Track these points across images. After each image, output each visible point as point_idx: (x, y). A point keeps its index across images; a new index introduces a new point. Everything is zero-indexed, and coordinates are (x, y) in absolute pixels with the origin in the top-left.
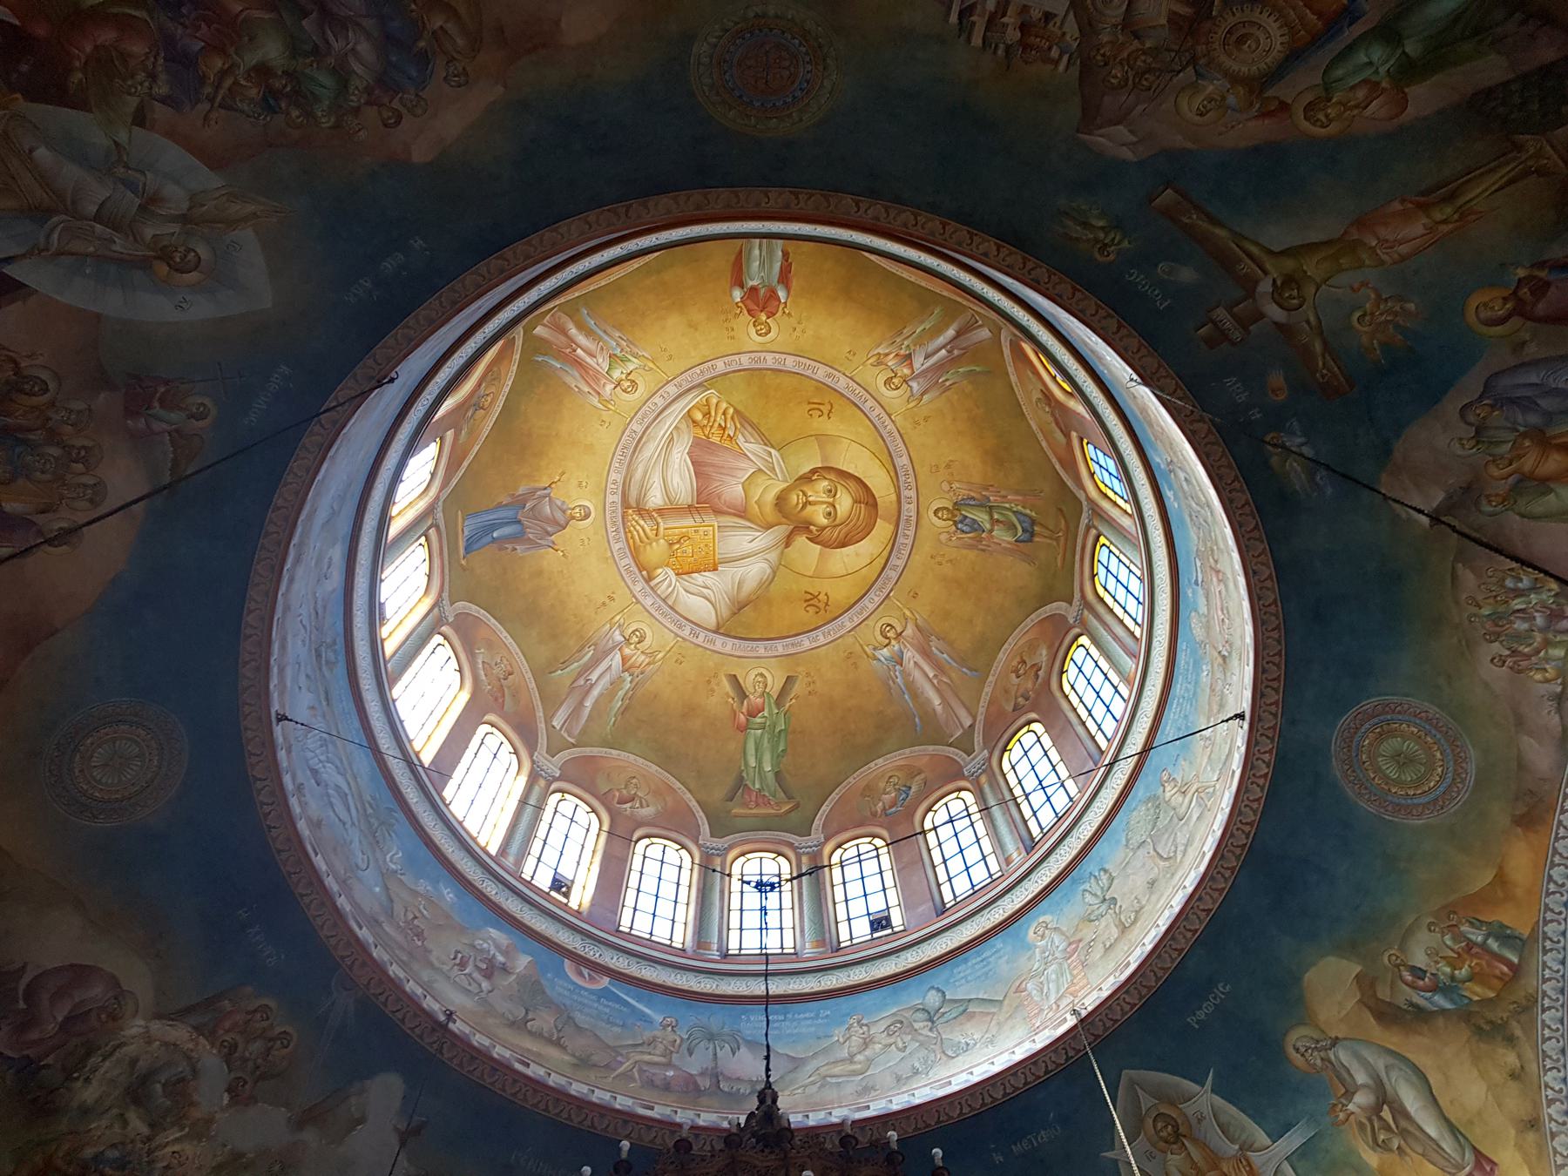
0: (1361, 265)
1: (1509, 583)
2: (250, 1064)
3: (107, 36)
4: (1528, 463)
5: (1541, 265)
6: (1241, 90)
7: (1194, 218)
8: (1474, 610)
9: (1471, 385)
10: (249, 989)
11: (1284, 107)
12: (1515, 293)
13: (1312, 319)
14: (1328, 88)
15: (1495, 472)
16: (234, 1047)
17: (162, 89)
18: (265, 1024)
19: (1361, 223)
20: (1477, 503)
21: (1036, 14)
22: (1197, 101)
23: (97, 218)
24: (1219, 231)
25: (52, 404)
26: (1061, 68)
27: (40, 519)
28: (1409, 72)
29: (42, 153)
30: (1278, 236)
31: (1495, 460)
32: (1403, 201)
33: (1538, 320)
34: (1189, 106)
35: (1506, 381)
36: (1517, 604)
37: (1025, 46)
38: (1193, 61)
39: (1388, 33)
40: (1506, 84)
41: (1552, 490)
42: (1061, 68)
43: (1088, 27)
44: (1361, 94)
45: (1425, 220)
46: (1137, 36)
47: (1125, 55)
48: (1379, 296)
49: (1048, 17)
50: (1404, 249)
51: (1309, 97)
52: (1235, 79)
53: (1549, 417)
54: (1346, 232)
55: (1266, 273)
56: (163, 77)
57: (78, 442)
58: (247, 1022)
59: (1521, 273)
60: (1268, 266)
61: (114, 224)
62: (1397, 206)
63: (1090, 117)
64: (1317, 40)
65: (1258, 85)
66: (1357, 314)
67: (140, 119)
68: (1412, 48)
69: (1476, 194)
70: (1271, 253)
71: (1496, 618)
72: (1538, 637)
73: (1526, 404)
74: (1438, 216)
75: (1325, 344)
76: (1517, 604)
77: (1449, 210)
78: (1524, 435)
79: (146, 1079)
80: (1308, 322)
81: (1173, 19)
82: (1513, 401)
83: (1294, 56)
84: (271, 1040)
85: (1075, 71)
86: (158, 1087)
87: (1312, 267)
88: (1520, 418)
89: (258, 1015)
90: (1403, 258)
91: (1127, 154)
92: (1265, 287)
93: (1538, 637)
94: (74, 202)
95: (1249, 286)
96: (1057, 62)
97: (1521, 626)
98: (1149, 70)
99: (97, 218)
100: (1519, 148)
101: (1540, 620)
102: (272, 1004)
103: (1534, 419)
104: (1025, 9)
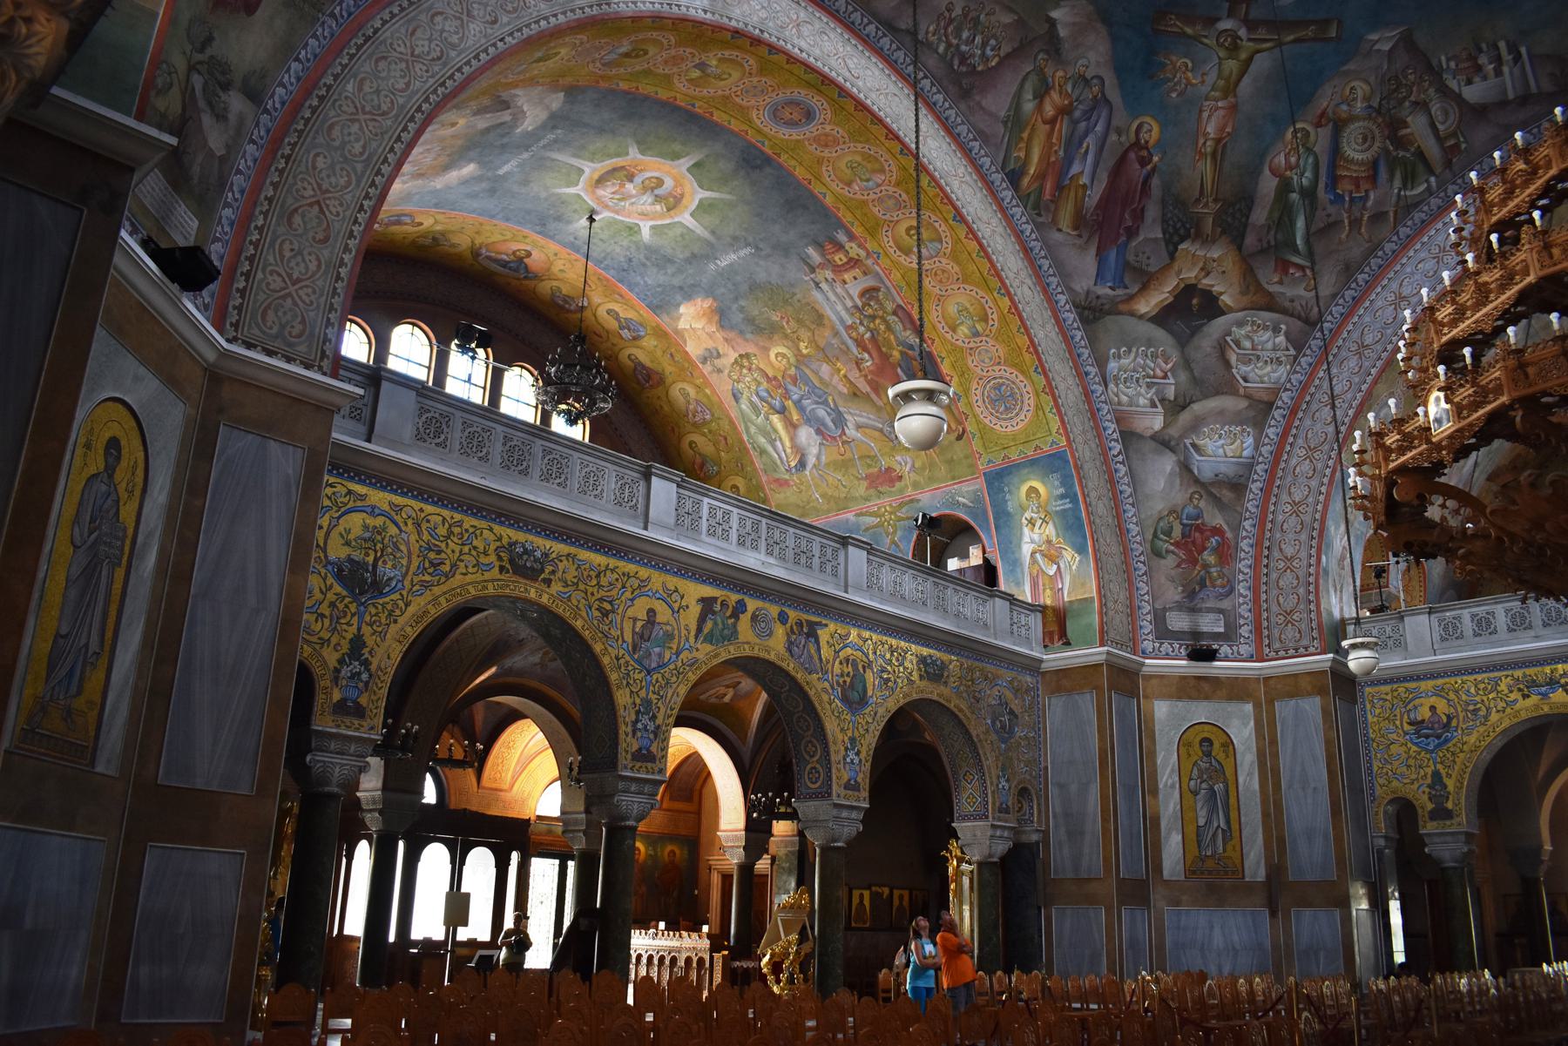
0: (1213, 89)
1: (993, 42)
4: (1055, 95)
5: (1154, 169)
6: (1344, 115)
7: (1310, 32)
8: (987, 9)
9: (1114, 95)
11: (1318, 125)
12: (1147, 148)
13: (1206, 41)
14: (1309, 150)
15: (1060, 73)
19: (1234, 108)
20: (1047, 52)
21: (1477, 79)
22: (1360, 93)
24: (1291, 37)
26: (1443, 58)
28: (1285, 187)
30: (1262, 63)
31: (1067, 79)
32: (1229, 134)
33: (1126, 152)
34: (1361, 88)
35: (1104, 114)
36: (978, 39)
37: (1473, 59)
38: (1379, 112)
39: (1309, 194)
40: (1248, 217)
41: (1035, 98)
42: (1443, 58)
43: (1444, 91)
44: (1293, 160)
45: (1212, 136)
46: (1416, 103)
47: (1415, 89)
48: (1192, 85)
49: (1469, 82)
50: (1205, 115)
51: (1312, 138)
52: (1352, 119)
53: (1075, 123)
54: (1235, 96)
55: (1250, 40)
59: (1156, 159)
60: (1251, 44)
62: (1228, 129)
63: (1407, 42)
64: (1333, 166)
65: (1339, 126)
66: (1190, 65)
68: (1294, 196)
69: (1207, 167)
70: (1258, 51)
71: (976, 21)
72: (955, 42)
73: (1088, 115)
74: (1208, 143)
75: (1189, 37)
76: (978, 39)
77: (1209, 149)
78: (1071, 104)
80: (1206, 37)
81: (1406, 125)
82: (1093, 109)
83: (1336, 151)
85: (1435, 63)
87: (1232, 65)
88: (1080, 107)
90: (1201, 111)
91: (1374, 37)
92: (1242, 32)
93: (955, 42)
95: (1251, 25)
96: (1448, 60)
97: (965, 35)
98: (1395, 90)
100: (1216, 200)
101: (963, 48)
103: (1077, 114)
104: (1485, 78)
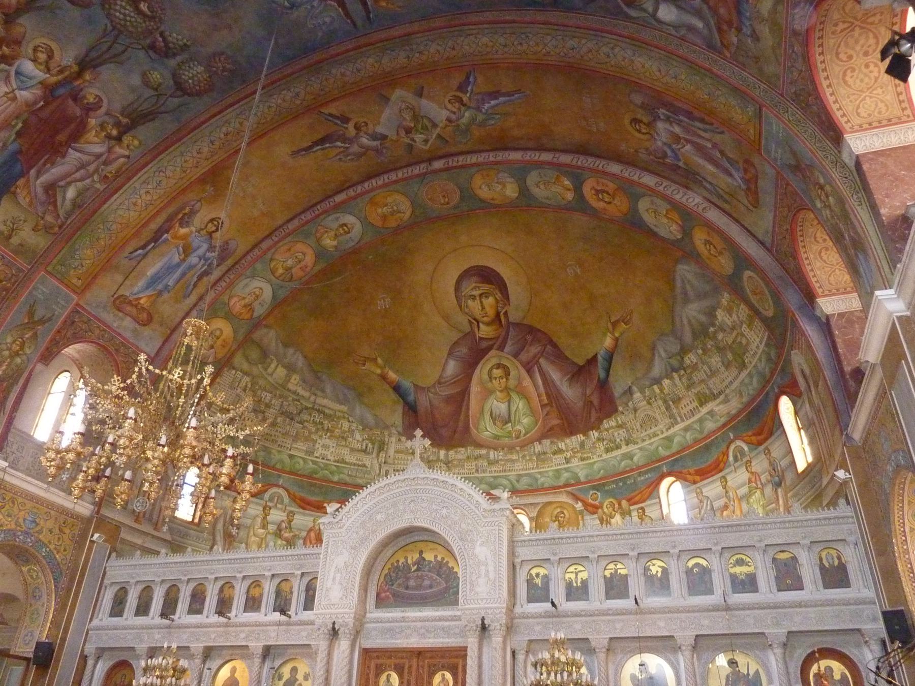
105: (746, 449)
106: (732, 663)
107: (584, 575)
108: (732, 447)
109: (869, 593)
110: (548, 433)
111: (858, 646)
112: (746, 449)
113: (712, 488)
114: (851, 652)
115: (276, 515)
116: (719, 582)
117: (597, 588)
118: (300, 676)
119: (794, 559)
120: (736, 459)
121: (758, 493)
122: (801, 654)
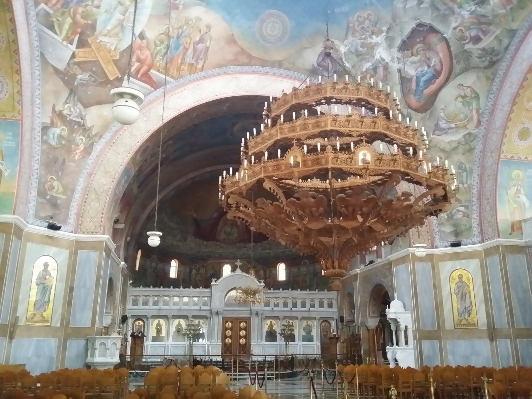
2: (371, 26)
3: (78, 17)
10: (351, 18)
16: (363, 28)
17: (90, 3)
18: (362, 18)
23: (124, 15)
25: (172, 27)
27: (202, 33)
29: (109, 28)
56: (87, 3)
57: (184, 22)
58: (359, 22)
61: (126, 11)
67: (98, 7)
79: (356, 50)
84: (367, 18)
86: (361, 49)
89: (359, 18)
94: (120, 20)
99: (124, 15)
102: (358, 14)
105: (308, 262)
106: (307, 322)
107: (278, 301)
108: (304, 260)
109: (336, 310)
110: (242, 241)
111: (331, 320)
112: (308, 262)
113: (295, 270)
114: (330, 321)
115: (154, 265)
116: (308, 305)
117: (281, 305)
118: (201, 323)
119: (323, 301)
120: (304, 264)
121: (309, 275)
122: (321, 321)
